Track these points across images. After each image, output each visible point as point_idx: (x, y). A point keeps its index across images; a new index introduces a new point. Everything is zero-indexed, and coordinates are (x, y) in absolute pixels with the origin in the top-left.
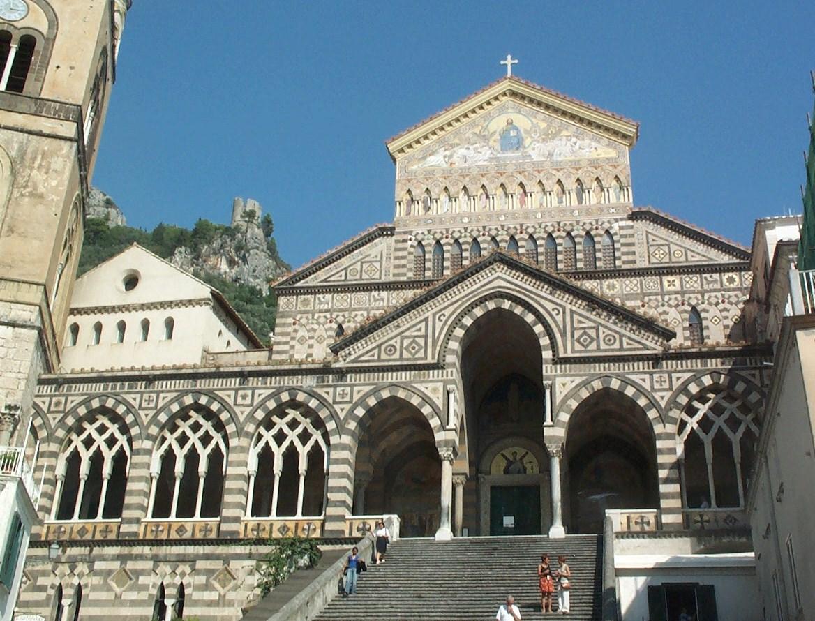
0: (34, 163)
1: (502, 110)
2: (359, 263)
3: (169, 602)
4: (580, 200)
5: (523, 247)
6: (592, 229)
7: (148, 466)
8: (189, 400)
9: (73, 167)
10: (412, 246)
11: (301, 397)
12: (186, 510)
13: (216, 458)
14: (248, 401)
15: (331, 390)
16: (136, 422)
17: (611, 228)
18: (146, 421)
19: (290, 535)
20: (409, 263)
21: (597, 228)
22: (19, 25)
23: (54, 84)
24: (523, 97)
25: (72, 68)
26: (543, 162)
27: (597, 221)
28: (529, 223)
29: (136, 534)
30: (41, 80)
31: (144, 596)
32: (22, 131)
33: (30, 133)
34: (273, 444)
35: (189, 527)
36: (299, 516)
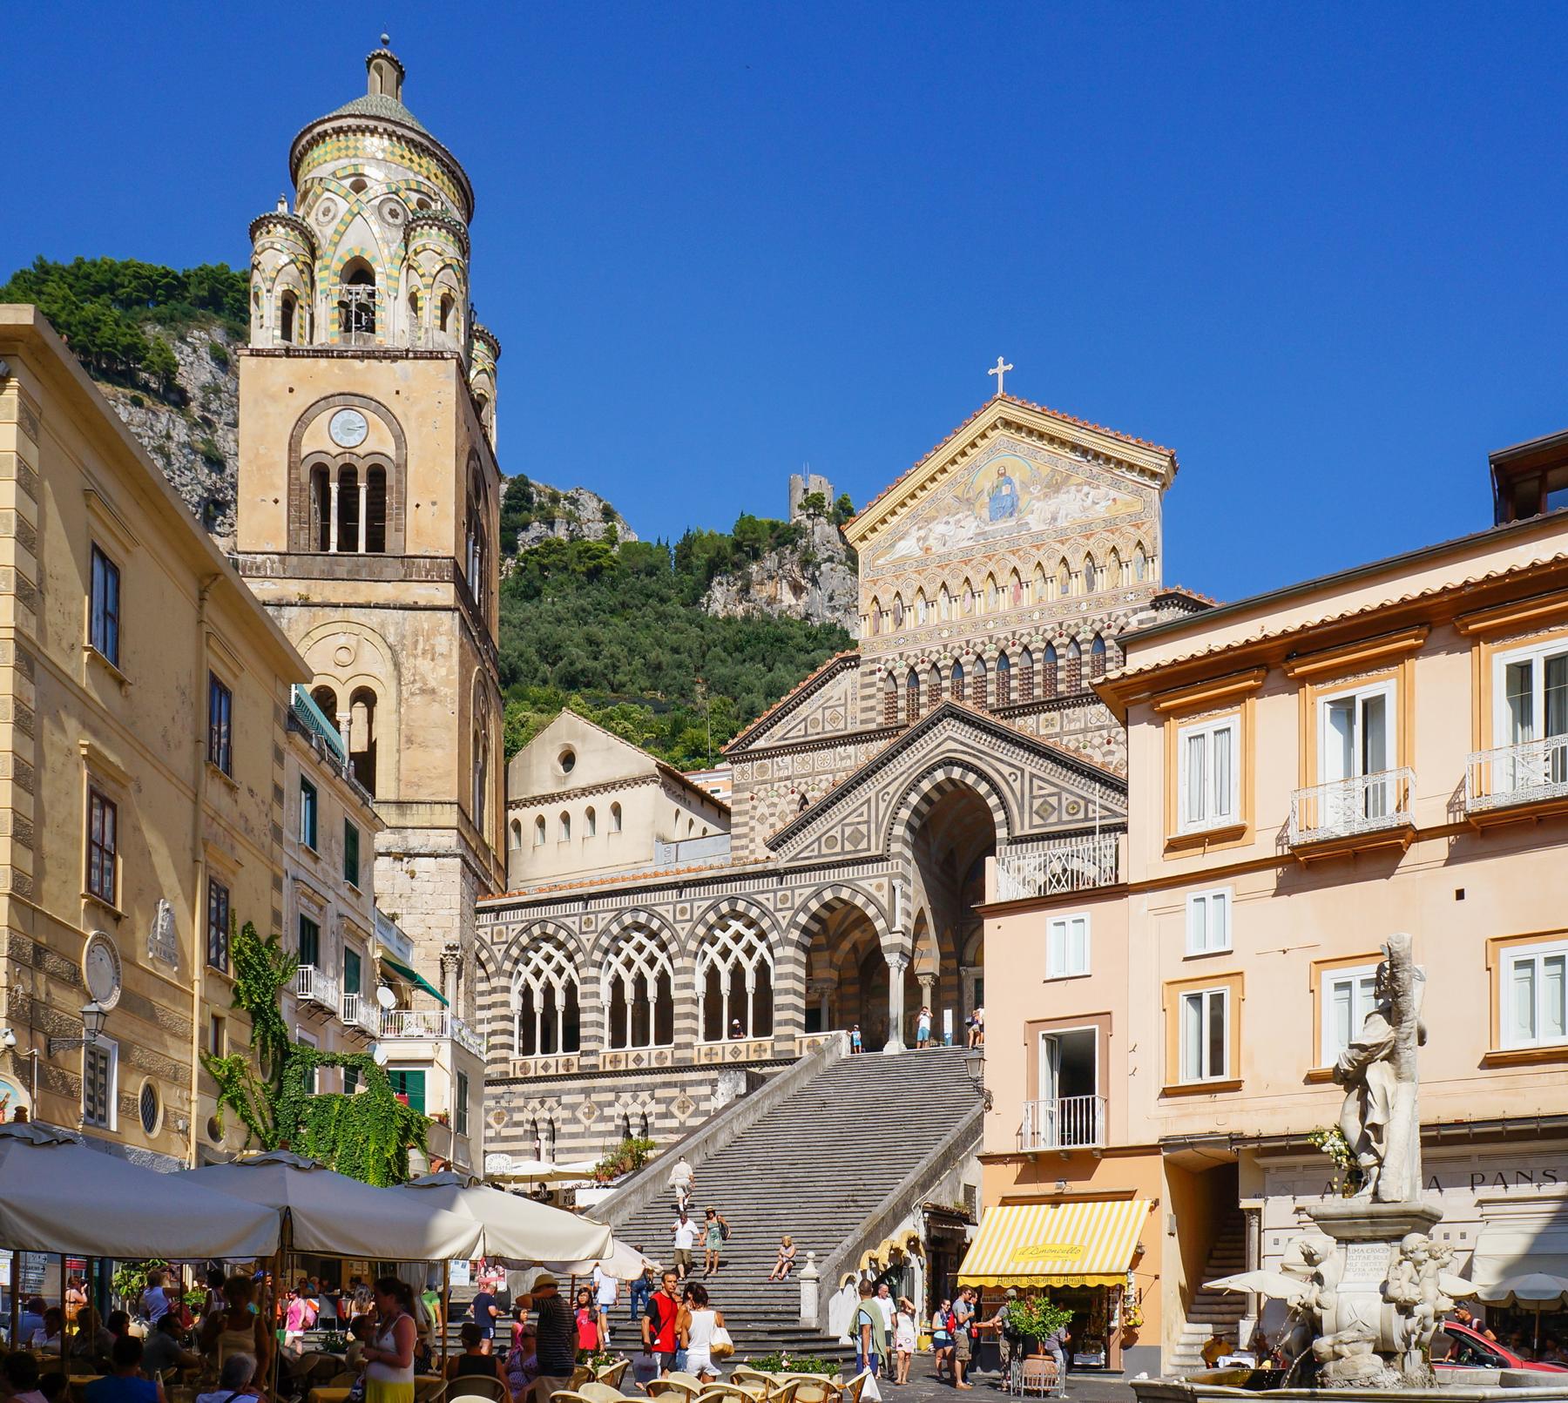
1: (993, 450)
3: (634, 1132)
4: (1091, 584)
5: (1015, 665)
6: (1102, 629)
7: (597, 995)
8: (628, 919)
9: (461, 646)
11: (741, 906)
12: (641, 1039)
13: (663, 980)
14: (688, 917)
15: (771, 895)
16: (578, 949)
17: (1128, 623)
18: (588, 946)
19: (742, 1058)
21: (1109, 627)
24: (1019, 428)
26: (1042, 533)
27: (1110, 615)
28: (1023, 629)
29: (596, 1066)
31: (611, 1126)
34: (719, 961)
35: (644, 1055)
36: (750, 1037)
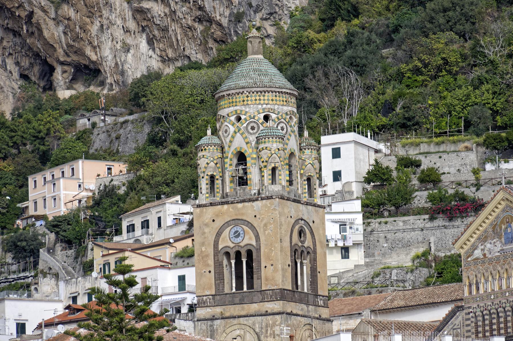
0: (267, 333)
2: (452, 330)
10: (472, 317)
20: (472, 329)
22: (242, 244)
23: (267, 279)
25: (272, 265)
30: (260, 278)
32: (258, 316)
33: (261, 315)
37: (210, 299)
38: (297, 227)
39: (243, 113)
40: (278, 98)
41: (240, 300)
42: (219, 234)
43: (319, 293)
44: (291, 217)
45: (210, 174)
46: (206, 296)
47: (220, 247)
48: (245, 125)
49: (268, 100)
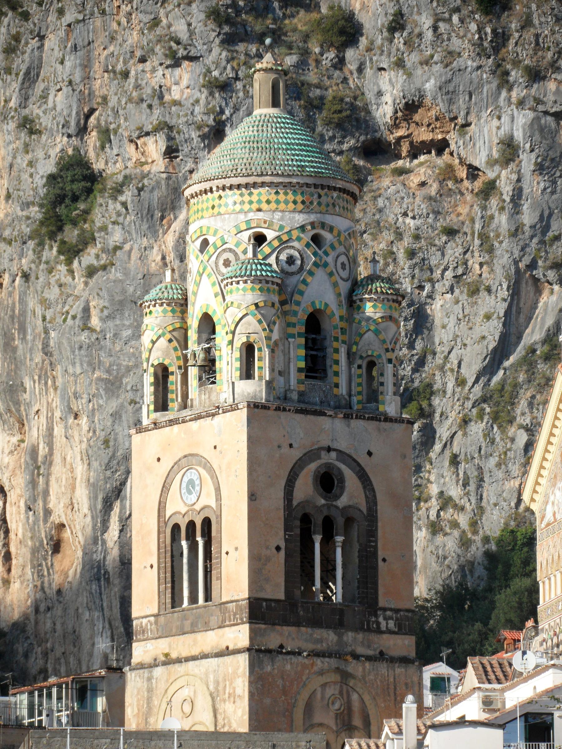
22: (198, 507)
37: (151, 625)
38: (313, 466)
39: (212, 231)
40: (282, 197)
41: (192, 624)
42: (165, 488)
43: (382, 602)
44: (291, 446)
45: (156, 363)
46: (146, 617)
47: (168, 514)
48: (214, 258)
49: (259, 202)
